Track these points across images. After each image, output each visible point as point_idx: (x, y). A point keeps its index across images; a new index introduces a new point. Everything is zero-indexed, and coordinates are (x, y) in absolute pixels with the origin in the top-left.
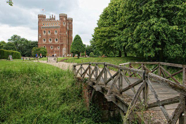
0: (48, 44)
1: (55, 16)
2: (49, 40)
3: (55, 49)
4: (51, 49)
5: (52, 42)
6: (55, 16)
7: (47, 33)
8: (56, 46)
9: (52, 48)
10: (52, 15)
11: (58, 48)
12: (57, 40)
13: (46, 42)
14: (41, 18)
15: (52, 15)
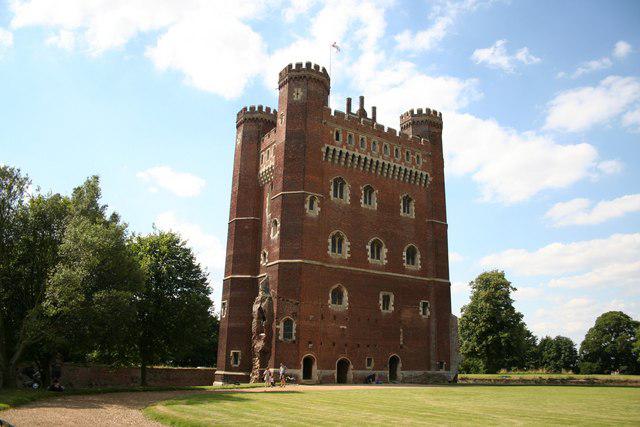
0: (369, 276)
1: (374, 109)
2: (369, 247)
3: (407, 314)
4: (386, 311)
5: (387, 268)
6: (374, 109)
7: (355, 198)
8: (409, 293)
9: (386, 299)
10: (362, 99)
11: (421, 309)
12: (411, 255)
13: (350, 261)
14: (307, 82)
15: (362, 99)
